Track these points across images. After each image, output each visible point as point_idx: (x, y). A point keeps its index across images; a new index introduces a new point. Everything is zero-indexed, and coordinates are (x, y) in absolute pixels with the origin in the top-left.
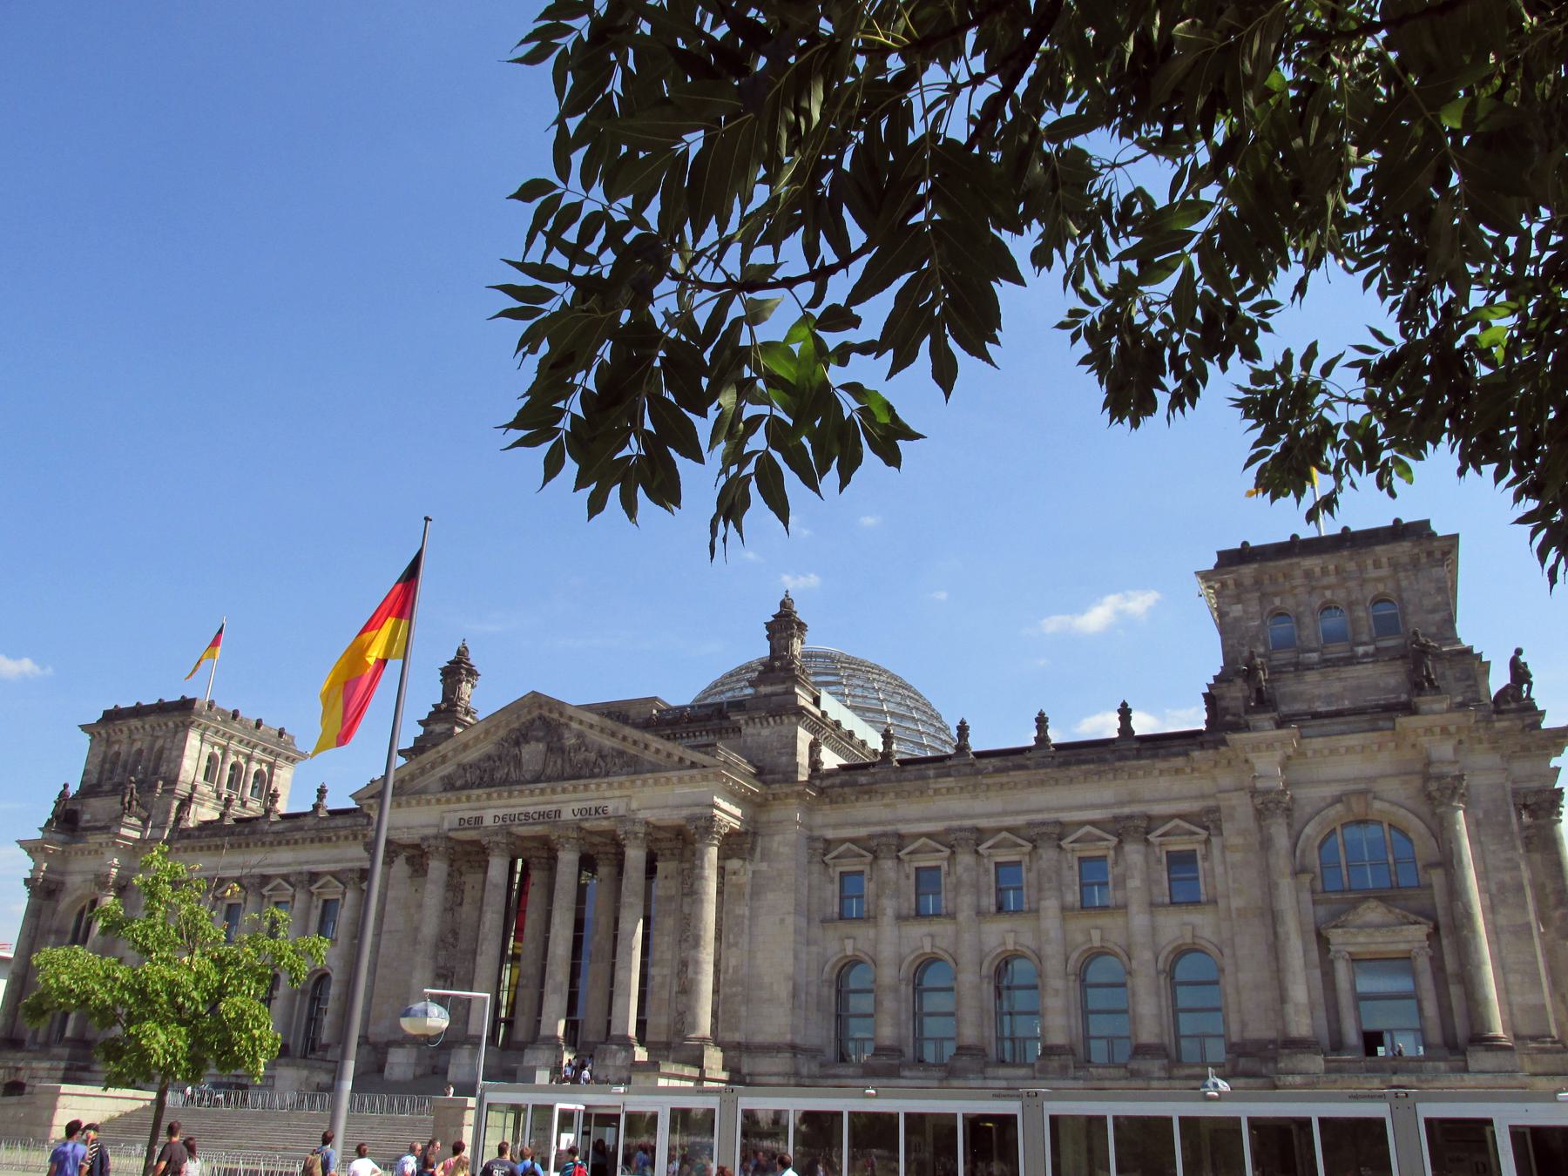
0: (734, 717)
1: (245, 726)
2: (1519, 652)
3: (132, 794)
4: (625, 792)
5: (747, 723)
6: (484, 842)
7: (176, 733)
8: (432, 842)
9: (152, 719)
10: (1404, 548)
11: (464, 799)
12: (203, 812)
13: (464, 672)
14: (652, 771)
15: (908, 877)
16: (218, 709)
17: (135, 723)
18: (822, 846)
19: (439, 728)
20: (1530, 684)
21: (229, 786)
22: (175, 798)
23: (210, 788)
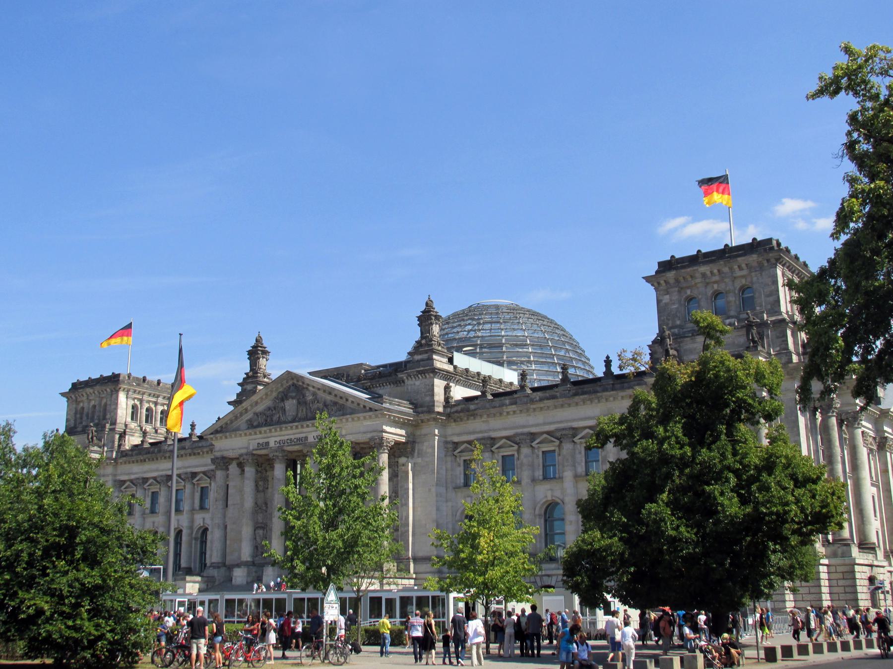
0: (400, 375)
1: (150, 384)
6: (271, 455)
7: (112, 395)
8: (245, 457)
9: (98, 388)
10: (753, 258)
12: (134, 440)
13: (260, 352)
14: (351, 414)
15: (498, 462)
16: (134, 378)
17: (89, 390)
18: (451, 446)
19: (249, 387)
21: (147, 421)
23: (136, 425)
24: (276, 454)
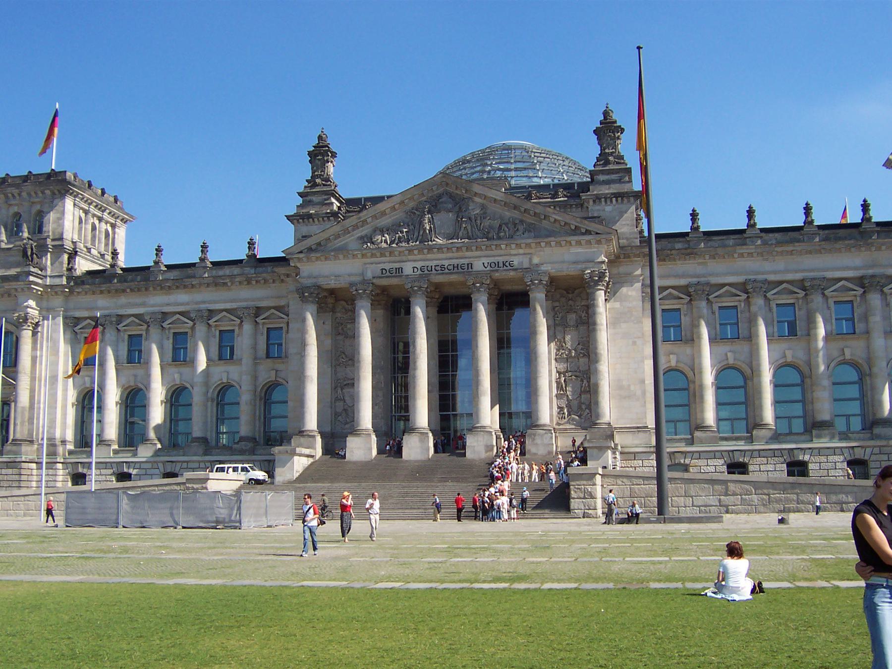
3: (32, 249)
4: (528, 251)
5: (594, 201)
15: (713, 313)
22: (65, 252)
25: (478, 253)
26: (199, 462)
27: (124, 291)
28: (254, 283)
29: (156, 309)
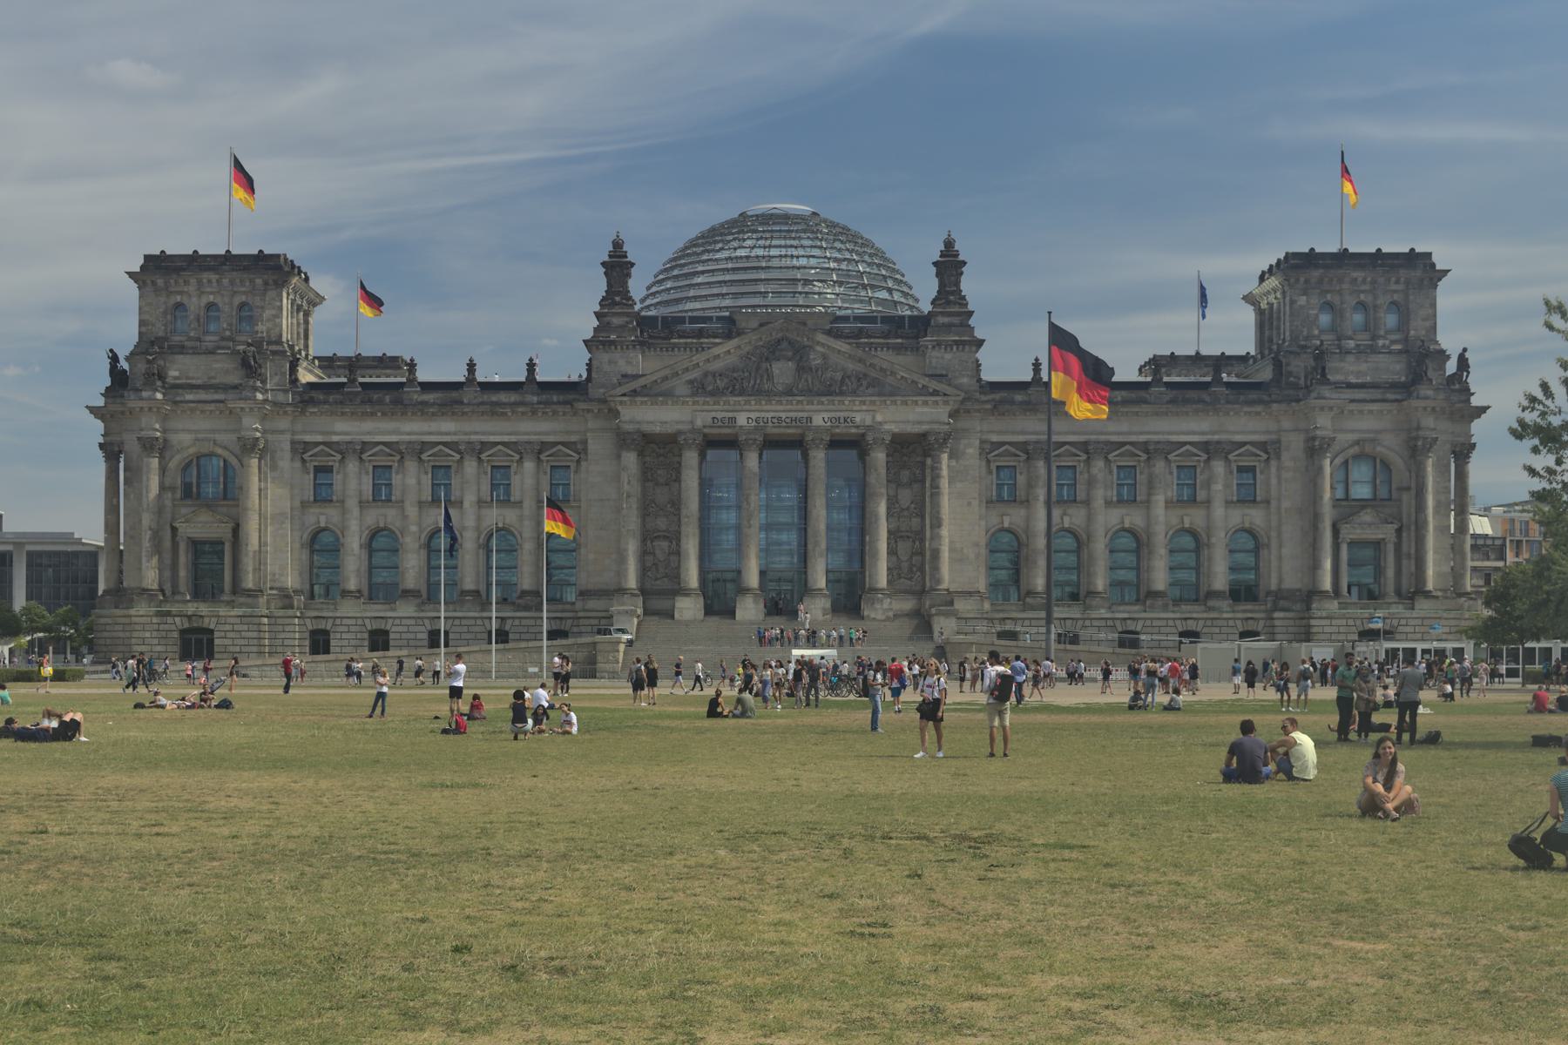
2: (1465, 350)
4: (874, 408)
5: (934, 347)
6: (742, 438)
10: (1417, 274)
11: (722, 403)
20: (1469, 373)
24: (752, 436)
25: (820, 407)
26: (475, 618)
27: (373, 414)
28: (540, 414)
29: (414, 438)
